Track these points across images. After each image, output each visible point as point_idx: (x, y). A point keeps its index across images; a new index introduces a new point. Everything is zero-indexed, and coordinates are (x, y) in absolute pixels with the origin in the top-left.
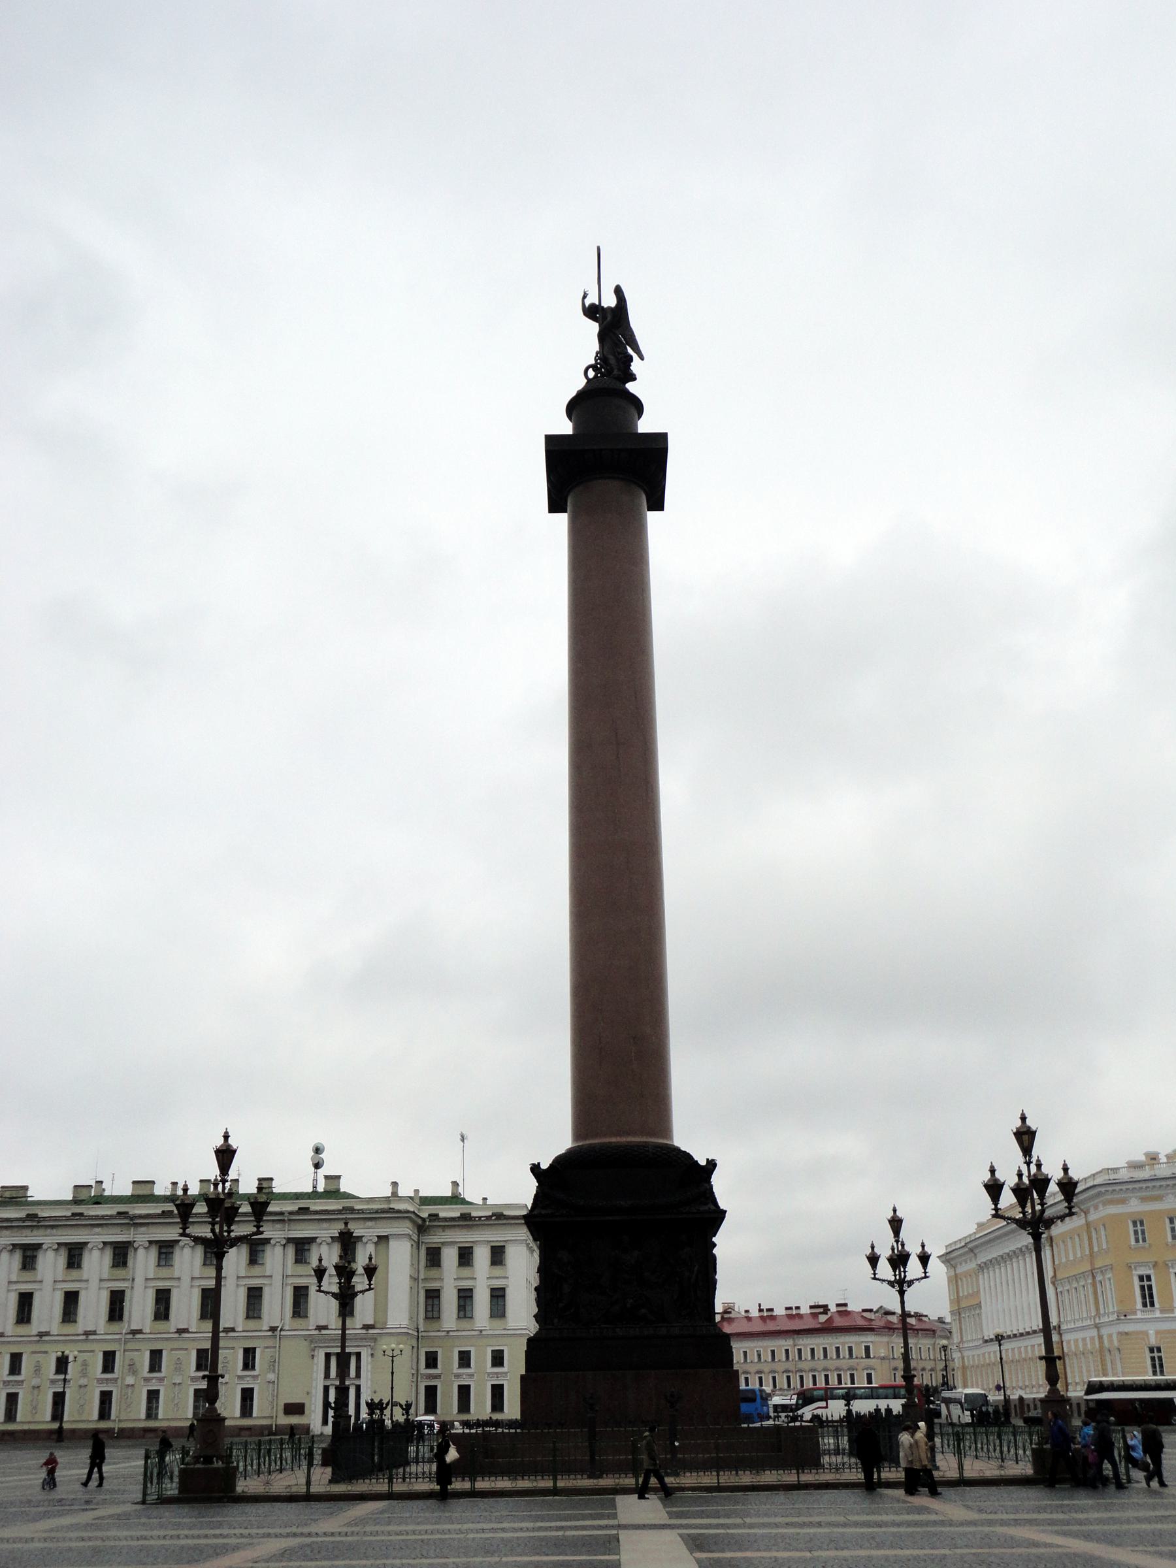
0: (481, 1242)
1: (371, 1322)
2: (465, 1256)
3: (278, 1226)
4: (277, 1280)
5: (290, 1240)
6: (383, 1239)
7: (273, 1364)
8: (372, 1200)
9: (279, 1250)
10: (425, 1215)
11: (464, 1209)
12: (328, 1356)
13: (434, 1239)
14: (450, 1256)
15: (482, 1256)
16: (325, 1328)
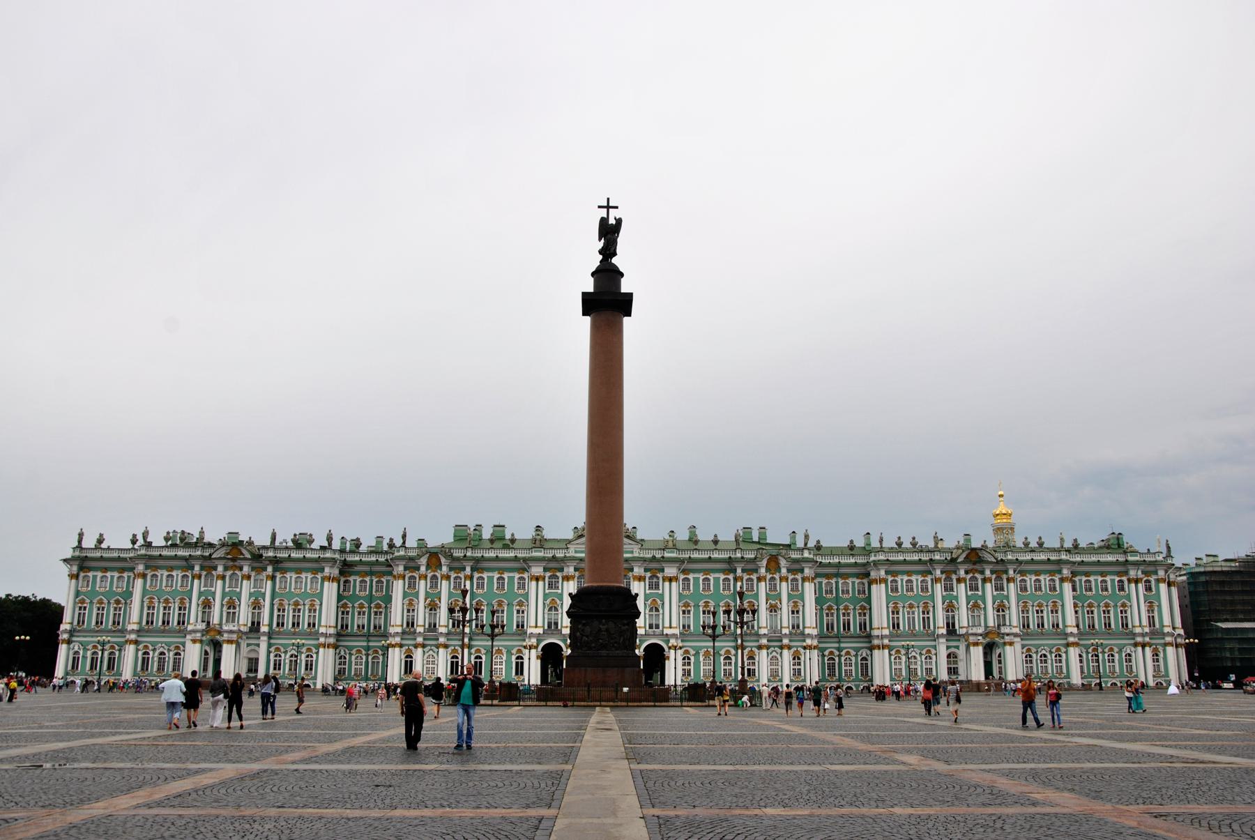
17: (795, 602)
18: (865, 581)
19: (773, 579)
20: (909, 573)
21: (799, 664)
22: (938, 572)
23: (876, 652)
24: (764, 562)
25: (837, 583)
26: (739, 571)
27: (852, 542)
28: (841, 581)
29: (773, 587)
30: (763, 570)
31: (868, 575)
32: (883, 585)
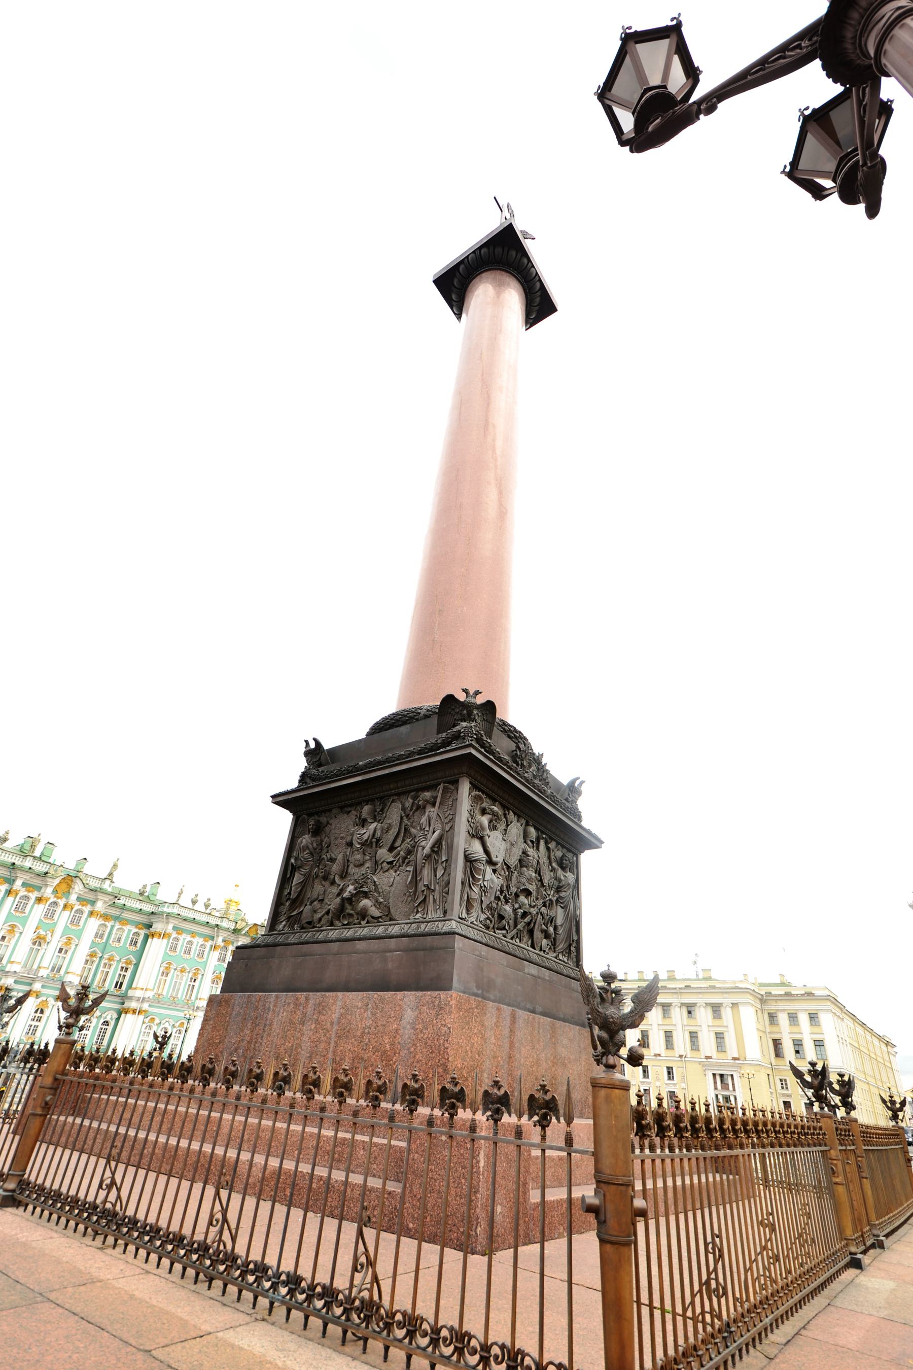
0: (803, 1010)
1: (736, 1056)
2: (793, 1018)
3: (675, 996)
4: (679, 1027)
5: (682, 1004)
6: (734, 1005)
7: (683, 1078)
8: (724, 982)
9: (677, 1009)
10: (763, 993)
11: (788, 989)
12: (714, 1075)
13: (772, 1007)
14: (783, 1019)
15: (803, 1018)
16: (710, 1058)
17: (69, 939)
18: (142, 932)
19: (55, 903)
20: (193, 934)
21: (39, 1020)
22: (220, 939)
23: (129, 1016)
24: (57, 881)
25: (113, 927)
26: (18, 883)
27: (145, 887)
28: (117, 926)
29: (49, 915)
30: (49, 890)
31: (149, 926)
32: (165, 941)
